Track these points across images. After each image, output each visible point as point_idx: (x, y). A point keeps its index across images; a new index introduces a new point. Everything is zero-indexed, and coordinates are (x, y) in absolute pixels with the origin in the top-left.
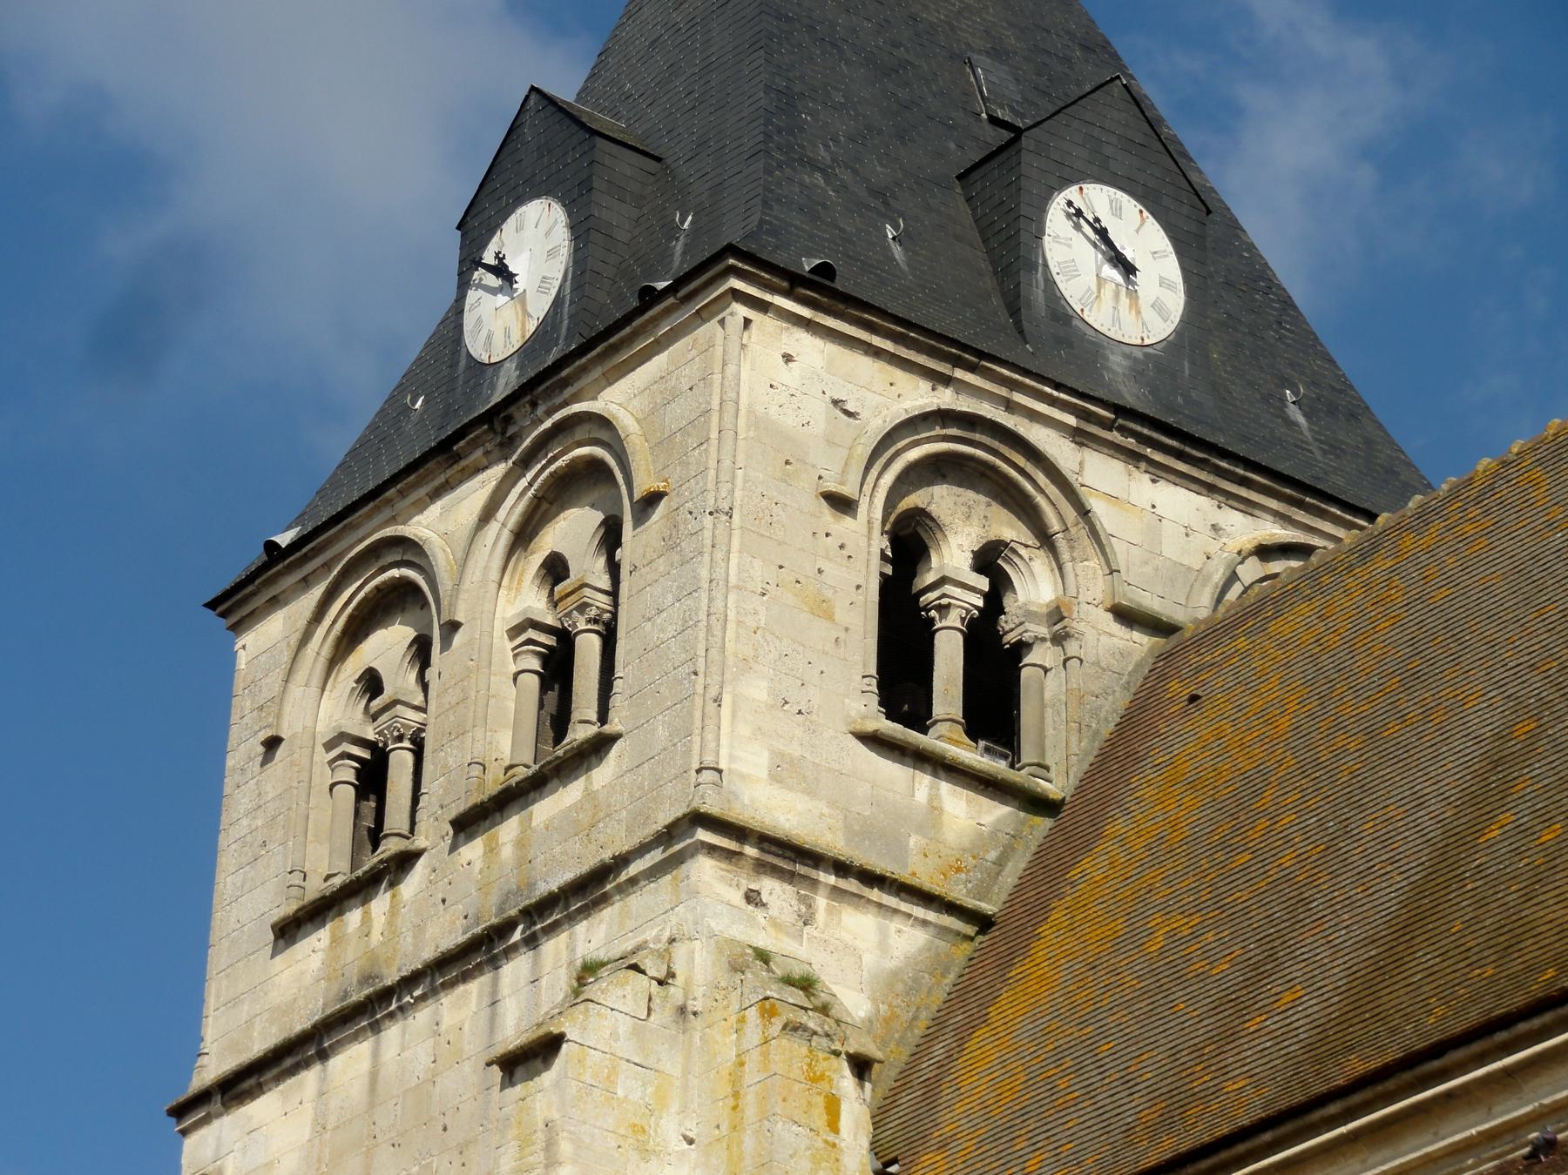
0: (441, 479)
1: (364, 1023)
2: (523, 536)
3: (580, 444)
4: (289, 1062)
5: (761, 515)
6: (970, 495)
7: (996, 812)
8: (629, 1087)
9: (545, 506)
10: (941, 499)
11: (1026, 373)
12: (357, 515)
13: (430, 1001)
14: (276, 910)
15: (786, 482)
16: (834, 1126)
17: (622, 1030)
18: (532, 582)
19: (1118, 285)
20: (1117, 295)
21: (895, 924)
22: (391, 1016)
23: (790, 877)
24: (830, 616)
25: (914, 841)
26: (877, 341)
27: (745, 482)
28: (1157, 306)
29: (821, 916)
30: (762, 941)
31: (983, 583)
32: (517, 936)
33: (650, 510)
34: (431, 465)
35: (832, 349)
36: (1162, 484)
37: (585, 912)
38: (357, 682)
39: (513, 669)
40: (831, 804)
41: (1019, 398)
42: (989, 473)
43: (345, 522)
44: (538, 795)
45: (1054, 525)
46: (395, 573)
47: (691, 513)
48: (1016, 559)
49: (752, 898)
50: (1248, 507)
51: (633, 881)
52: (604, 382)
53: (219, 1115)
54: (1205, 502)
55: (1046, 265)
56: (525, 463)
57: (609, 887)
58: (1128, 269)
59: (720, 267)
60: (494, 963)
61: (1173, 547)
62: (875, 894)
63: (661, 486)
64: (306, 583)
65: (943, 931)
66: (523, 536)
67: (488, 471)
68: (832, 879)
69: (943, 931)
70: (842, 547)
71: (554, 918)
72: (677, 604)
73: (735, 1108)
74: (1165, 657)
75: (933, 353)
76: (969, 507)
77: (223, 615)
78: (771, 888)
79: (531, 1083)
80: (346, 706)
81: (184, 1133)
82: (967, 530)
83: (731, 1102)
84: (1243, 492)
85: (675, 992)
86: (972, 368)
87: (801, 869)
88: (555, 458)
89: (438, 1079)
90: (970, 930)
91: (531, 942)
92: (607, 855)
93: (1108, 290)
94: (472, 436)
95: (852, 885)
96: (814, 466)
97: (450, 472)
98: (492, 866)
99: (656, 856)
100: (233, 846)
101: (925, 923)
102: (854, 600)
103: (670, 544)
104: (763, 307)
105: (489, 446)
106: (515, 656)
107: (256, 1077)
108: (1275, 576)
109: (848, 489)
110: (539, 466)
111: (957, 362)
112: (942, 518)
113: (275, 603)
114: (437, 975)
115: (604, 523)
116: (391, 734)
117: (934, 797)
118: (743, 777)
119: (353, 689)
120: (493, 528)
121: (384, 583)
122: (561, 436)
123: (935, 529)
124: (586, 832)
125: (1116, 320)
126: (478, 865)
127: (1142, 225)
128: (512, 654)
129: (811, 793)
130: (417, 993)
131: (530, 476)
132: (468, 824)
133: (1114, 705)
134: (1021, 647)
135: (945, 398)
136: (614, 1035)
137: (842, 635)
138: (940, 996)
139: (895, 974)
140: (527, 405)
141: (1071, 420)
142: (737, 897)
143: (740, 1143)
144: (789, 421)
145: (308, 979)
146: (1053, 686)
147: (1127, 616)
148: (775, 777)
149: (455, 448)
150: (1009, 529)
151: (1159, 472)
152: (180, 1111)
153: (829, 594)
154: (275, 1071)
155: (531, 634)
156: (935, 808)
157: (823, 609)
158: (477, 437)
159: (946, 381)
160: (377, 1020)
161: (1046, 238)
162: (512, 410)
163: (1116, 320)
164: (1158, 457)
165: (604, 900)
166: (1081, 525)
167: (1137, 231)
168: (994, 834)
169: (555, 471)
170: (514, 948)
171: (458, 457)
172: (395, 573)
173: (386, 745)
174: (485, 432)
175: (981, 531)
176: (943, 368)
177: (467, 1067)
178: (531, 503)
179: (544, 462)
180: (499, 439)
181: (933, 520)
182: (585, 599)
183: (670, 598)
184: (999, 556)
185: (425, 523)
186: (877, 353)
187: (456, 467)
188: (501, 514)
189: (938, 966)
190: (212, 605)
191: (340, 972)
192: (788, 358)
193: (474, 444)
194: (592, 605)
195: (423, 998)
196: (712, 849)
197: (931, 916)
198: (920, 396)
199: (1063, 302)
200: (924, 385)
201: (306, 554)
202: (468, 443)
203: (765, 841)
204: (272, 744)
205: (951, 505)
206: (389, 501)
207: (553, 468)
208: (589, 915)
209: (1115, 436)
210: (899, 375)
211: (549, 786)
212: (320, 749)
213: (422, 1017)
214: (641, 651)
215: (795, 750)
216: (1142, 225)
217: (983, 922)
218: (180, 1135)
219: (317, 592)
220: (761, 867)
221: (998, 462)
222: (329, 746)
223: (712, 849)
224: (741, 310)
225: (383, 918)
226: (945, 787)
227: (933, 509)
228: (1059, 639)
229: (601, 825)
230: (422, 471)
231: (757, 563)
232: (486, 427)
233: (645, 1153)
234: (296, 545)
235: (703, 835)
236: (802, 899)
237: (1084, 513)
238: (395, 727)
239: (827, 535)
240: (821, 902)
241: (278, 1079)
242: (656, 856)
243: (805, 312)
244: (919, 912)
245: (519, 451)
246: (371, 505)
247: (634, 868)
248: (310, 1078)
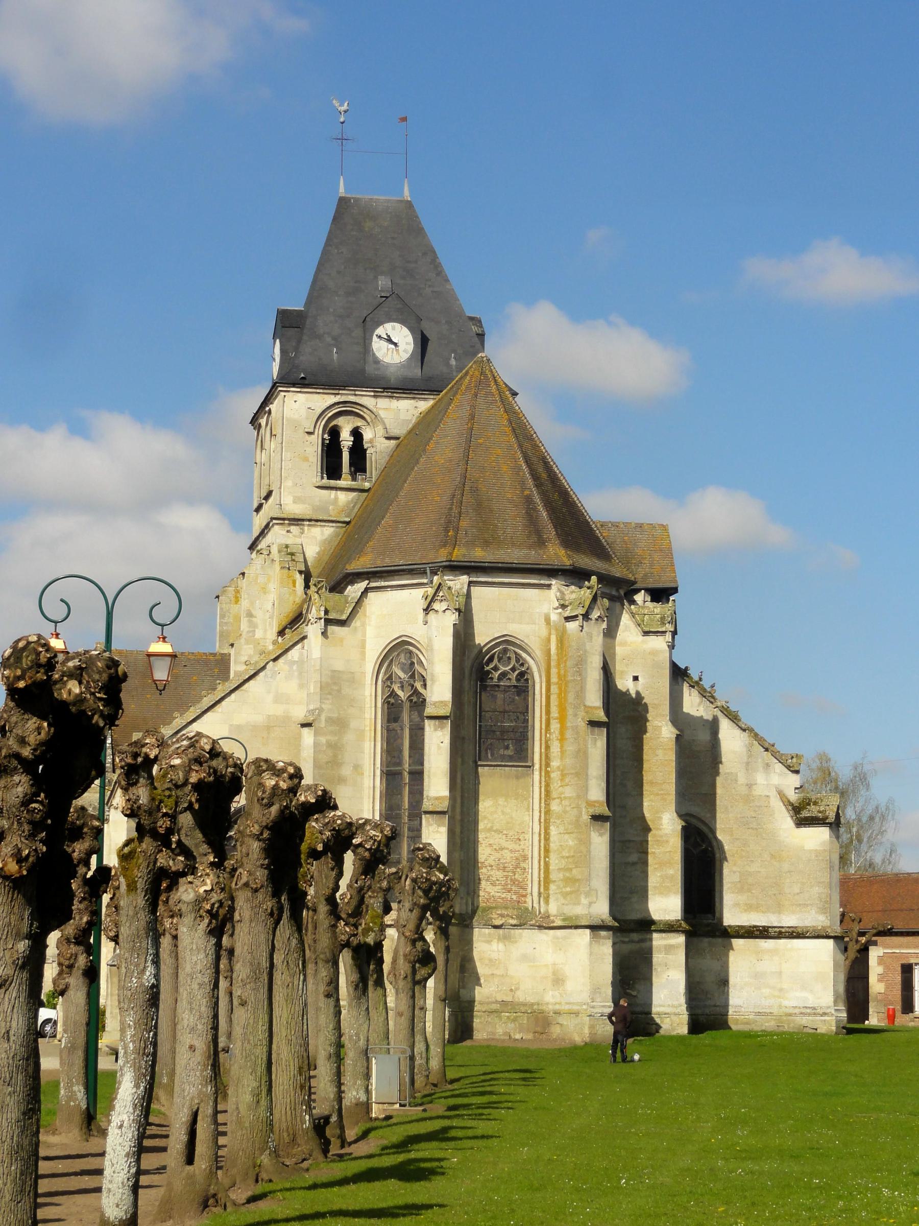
6: (349, 417)
7: (353, 495)
8: (261, 580)
10: (341, 421)
16: (295, 586)
20: (393, 352)
21: (326, 528)
23: (298, 525)
26: (318, 391)
28: (405, 351)
30: (289, 542)
40: (309, 504)
41: (357, 393)
45: (369, 420)
49: (288, 531)
50: (425, 399)
54: (412, 401)
58: (395, 344)
61: (403, 416)
62: (319, 523)
65: (337, 527)
68: (308, 523)
69: (337, 527)
74: (398, 446)
75: (333, 389)
78: (293, 528)
84: (423, 396)
86: (344, 390)
87: (299, 523)
90: (344, 525)
93: (390, 352)
95: (313, 523)
104: (288, 391)
109: (311, 430)
111: (340, 389)
117: (336, 494)
118: (286, 504)
125: (392, 358)
129: (304, 503)
134: (366, 450)
139: (326, 540)
141: (372, 394)
142: (284, 532)
147: (388, 438)
148: (294, 502)
150: (359, 423)
156: (336, 498)
157: (306, 459)
159: (338, 394)
163: (392, 358)
164: (398, 395)
168: (352, 500)
176: (336, 392)
186: (319, 393)
196: (277, 524)
197: (334, 525)
198: (332, 399)
203: (289, 519)
209: (385, 394)
215: (300, 495)
217: (348, 523)
220: (289, 525)
223: (277, 524)
226: (339, 492)
227: (339, 424)
233: (265, 593)
235: (274, 521)
240: (306, 528)
243: (299, 390)
244: (331, 524)
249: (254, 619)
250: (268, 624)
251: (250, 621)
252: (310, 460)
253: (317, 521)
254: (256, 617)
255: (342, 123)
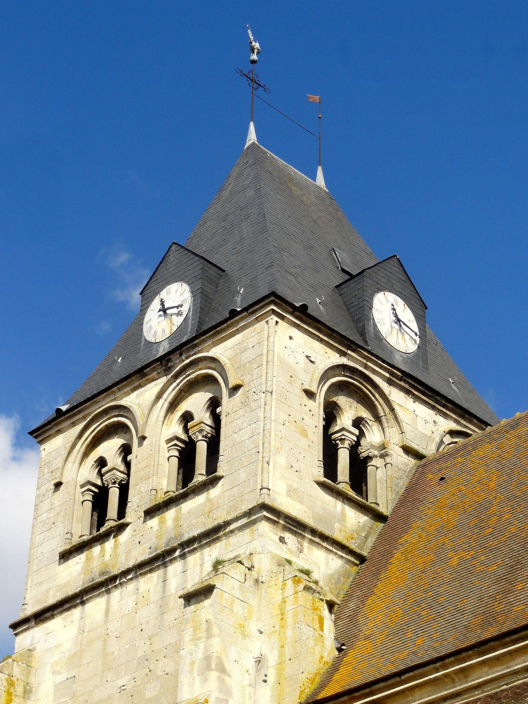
0: (138, 383)
1: (104, 589)
2: (173, 406)
3: (200, 369)
4: (67, 606)
5: (282, 395)
7: (364, 519)
9: (183, 393)
10: (342, 400)
11: (373, 355)
12: (99, 397)
13: (134, 580)
14: (60, 548)
15: (291, 383)
17: (236, 586)
18: (177, 422)
19: (398, 330)
21: (331, 556)
22: (116, 587)
24: (306, 436)
25: (337, 525)
27: (277, 381)
29: (306, 550)
31: (357, 432)
32: (177, 553)
33: (235, 392)
34: (133, 378)
35: (306, 337)
36: (417, 403)
37: (208, 544)
38: (95, 462)
39: (168, 455)
40: (308, 507)
42: (358, 391)
43: (93, 400)
44: (184, 501)
46: (115, 419)
47: (254, 392)
48: (367, 425)
50: (445, 416)
51: (232, 532)
52: (212, 346)
53: (33, 627)
54: (432, 412)
55: (373, 319)
56: (176, 377)
57: (222, 533)
59: (269, 300)
60: (165, 565)
61: (421, 427)
63: (240, 382)
64: (74, 424)
65: (349, 561)
66: (173, 406)
67: (158, 380)
69: (349, 561)
70: (310, 411)
71: (195, 546)
72: (249, 427)
73: (282, 619)
76: (351, 403)
77: (36, 437)
78: (288, 536)
79: (199, 605)
80: (90, 471)
81: (16, 635)
82: (350, 411)
83: (280, 617)
85: (254, 573)
86: (354, 351)
88: (189, 375)
89: (138, 611)
91: (183, 556)
92: (221, 521)
93: (395, 331)
94: (153, 366)
95: (317, 540)
96: (300, 379)
97: (141, 381)
98: (162, 528)
99: (244, 521)
100: (39, 524)
101: (342, 557)
102: (314, 431)
103: (245, 404)
104: (282, 318)
105: (159, 371)
106: (169, 450)
107: (51, 612)
108: (456, 443)
110: (182, 378)
112: (342, 406)
113: (59, 432)
114: (138, 570)
115: (211, 399)
116: (111, 481)
117: (343, 510)
119: (93, 465)
120: (161, 401)
121: (109, 423)
122: (192, 367)
123: (339, 410)
124: (207, 514)
126: (156, 528)
127: (405, 309)
128: (167, 450)
129: (301, 502)
130: (128, 577)
131: (178, 381)
132: (150, 513)
133: (404, 483)
134: (369, 458)
135: (344, 361)
136: (233, 588)
137: (311, 444)
138: (346, 587)
139: (331, 576)
140: (178, 355)
141: (387, 375)
143: (285, 633)
144: (292, 361)
145: (75, 574)
146: (380, 474)
147: (408, 450)
149: (145, 371)
150: (365, 414)
151: (416, 398)
152: (14, 626)
153: (306, 428)
154: (60, 609)
155: (176, 442)
156: (343, 514)
157: (304, 433)
158: (155, 367)
160: (109, 589)
161: (373, 309)
162: (172, 356)
163: (397, 342)
164: (416, 393)
165: (218, 539)
166: (390, 414)
167: (403, 311)
168: (364, 525)
169: (189, 380)
170: (175, 558)
171: (146, 375)
172: (115, 419)
173: (108, 485)
174: (158, 365)
175: (355, 413)
177: (152, 606)
178: (178, 392)
179: (184, 376)
180: (164, 368)
181: (339, 407)
182: (202, 428)
183: (245, 425)
184: (360, 423)
185: (129, 400)
186: (321, 341)
187: (144, 379)
188: (165, 396)
189: (346, 575)
190: (31, 433)
191: (90, 571)
192: (291, 338)
193: (153, 370)
194: (205, 430)
195: (131, 579)
196: (268, 519)
198: (336, 359)
199: (379, 333)
200: (337, 355)
201: (75, 413)
202: (151, 369)
204: (58, 485)
205: (345, 402)
206: (114, 393)
207: (188, 378)
208: (210, 545)
209: (402, 384)
210: (329, 350)
211: (189, 497)
212: (78, 487)
213: (131, 587)
214: (232, 445)
215: (295, 485)
216: (405, 309)
217: (362, 559)
218: (14, 636)
219: (79, 427)
220: (285, 528)
221: (362, 387)
222: (82, 486)
224: (275, 318)
225: (111, 550)
227: (339, 402)
228: (382, 456)
229: (214, 511)
230: (129, 380)
231: (281, 412)
232: (159, 363)
234: (68, 411)
235: (265, 513)
236: (299, 543)
237: (392, 410)
238: (113, 478)
239: (305, 406)
241: (61, 613)
242: (244, 521)
245: (174, 372)
246: (106, 394)
247: (232, 527)
248: (76, 613)
249: (226, 678)
250: (247, 696)
251: (221, 681)
252: (310, 436)
253: (324, 537)
254: (229, 676)
255: (253, 62)
